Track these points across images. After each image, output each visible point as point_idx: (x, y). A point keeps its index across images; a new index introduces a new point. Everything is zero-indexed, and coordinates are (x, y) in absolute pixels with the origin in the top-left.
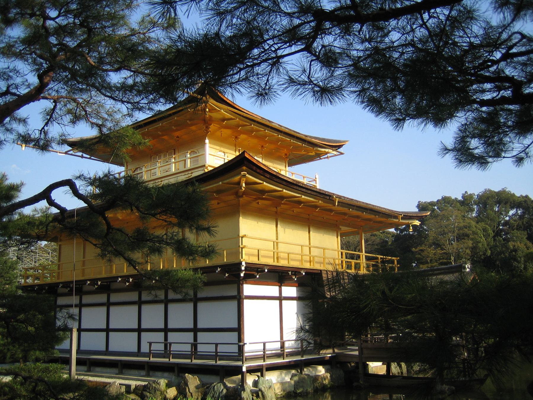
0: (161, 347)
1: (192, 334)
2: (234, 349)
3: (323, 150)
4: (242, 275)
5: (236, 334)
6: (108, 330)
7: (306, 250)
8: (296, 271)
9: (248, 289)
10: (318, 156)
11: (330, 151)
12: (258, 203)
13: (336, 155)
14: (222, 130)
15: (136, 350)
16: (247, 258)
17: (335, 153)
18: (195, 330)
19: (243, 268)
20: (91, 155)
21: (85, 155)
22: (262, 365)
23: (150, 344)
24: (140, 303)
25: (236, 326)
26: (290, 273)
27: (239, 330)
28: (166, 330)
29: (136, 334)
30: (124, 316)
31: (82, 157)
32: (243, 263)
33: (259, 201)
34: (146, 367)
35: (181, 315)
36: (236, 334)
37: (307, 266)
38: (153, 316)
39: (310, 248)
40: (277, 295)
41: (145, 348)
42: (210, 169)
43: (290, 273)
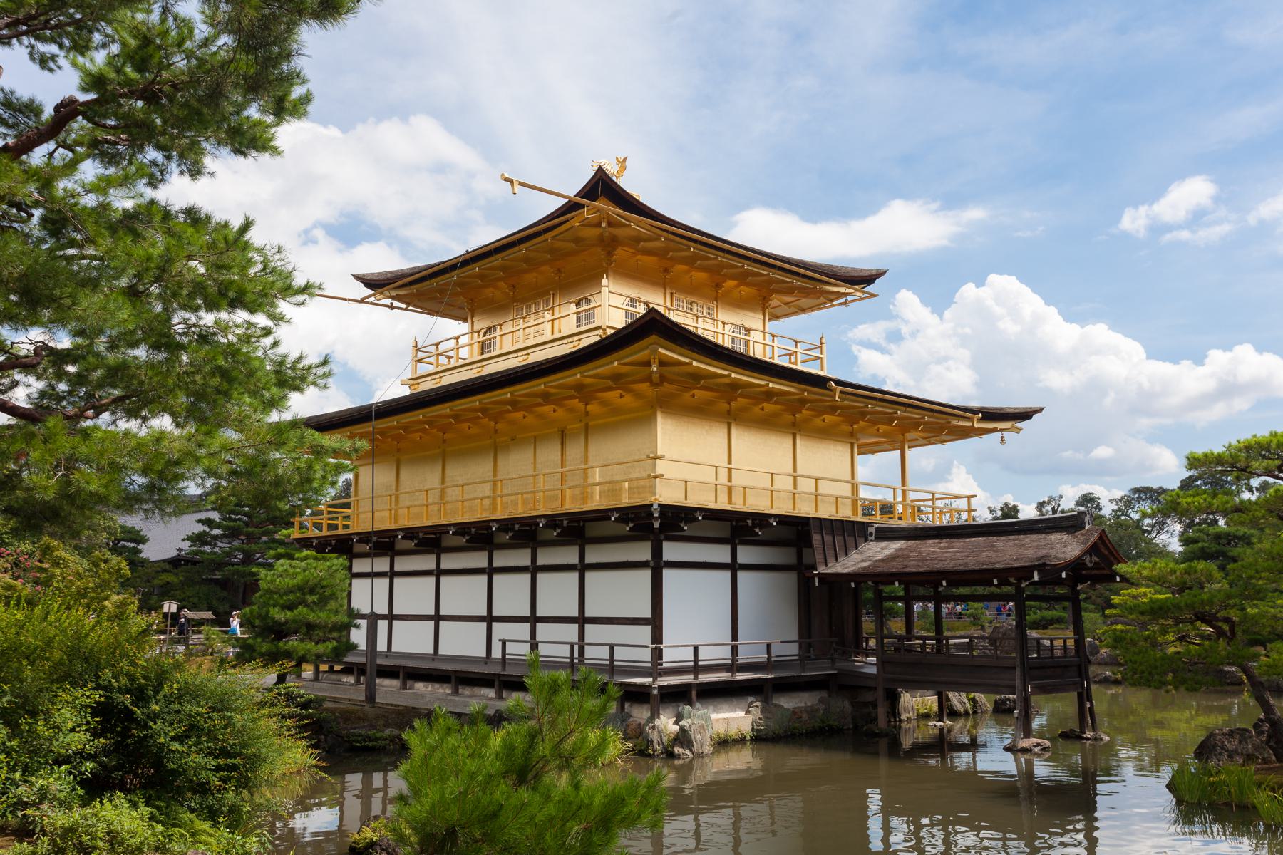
1: (575, 627)
2: (645, 655)
3: (835, 289)
4: (656, 525)
5: (648, 629)
6: (437, 618)
8: (761, 519)
9: (671, 551)
10: (831, 298)
11: (849, 290)
12: (693, 396)
13: (861, 299)
14: (639, 257)
15: (482, 653)
16: (667, 495)
17: (860, 294)
19: (656, 515)
20: (408, 304)
21: (396, 304)
22: (689, 686)
23: (504, 643)
24: (491, 571)
25: (647, 613)
26: (750, 522)
27: (655, 621)
28: (534, 619)
29: (484, 625)
30: (464, 594)
31: (392, 307)
32: (655, 506)
33: (695, 391)
34: (496, 683)
35: (558, 594)
36: (648, 629)
37: (783, 507)
38: (512, 594)
39: (795, 478)
40: (727, 559)
41: (497, 653)
42: (610, 332)
43: (750, 522)
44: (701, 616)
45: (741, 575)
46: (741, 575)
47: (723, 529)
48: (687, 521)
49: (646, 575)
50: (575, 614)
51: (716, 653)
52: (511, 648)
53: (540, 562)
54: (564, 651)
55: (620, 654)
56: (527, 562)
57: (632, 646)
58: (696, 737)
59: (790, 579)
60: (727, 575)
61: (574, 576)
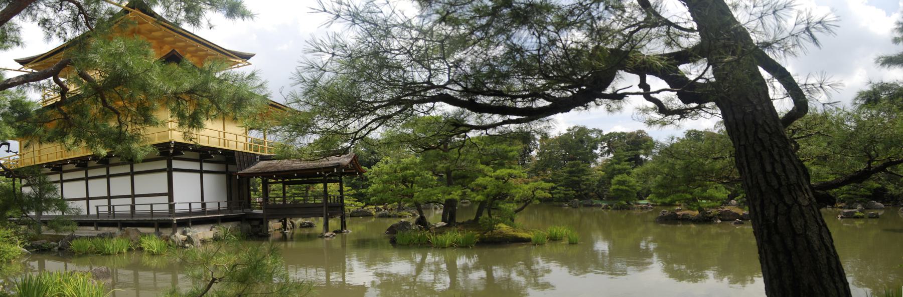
0: (106, 209)
2: (166, 207)
4: (171, 151)
5: (167, 197)
7: (222, 134)
8: (215, 150)
9: (176, 164)
18: (133, 196)
23: (97, 207)
25: (166, 191)
27: (170, 194)
28: (109, 197)
36: (167, 197)
37: (222, 147)
38: (98, 187)
41: (93, 212)
44: (190, 190)
45: (204, 175)
46: (204, 175)
47: (196, 155)
48: (184, 150)
49: (165, 175)
50: (130, 194)
51: (197, 207)
52: (100, 209)
53: (111, 173)
54: (129, 208)
55: (155, 208)
56: (105, 173)
57: (161, 206)
58: (195, 240)
59: (223, 178)
60: (198, 175)
61: (129, 178)
